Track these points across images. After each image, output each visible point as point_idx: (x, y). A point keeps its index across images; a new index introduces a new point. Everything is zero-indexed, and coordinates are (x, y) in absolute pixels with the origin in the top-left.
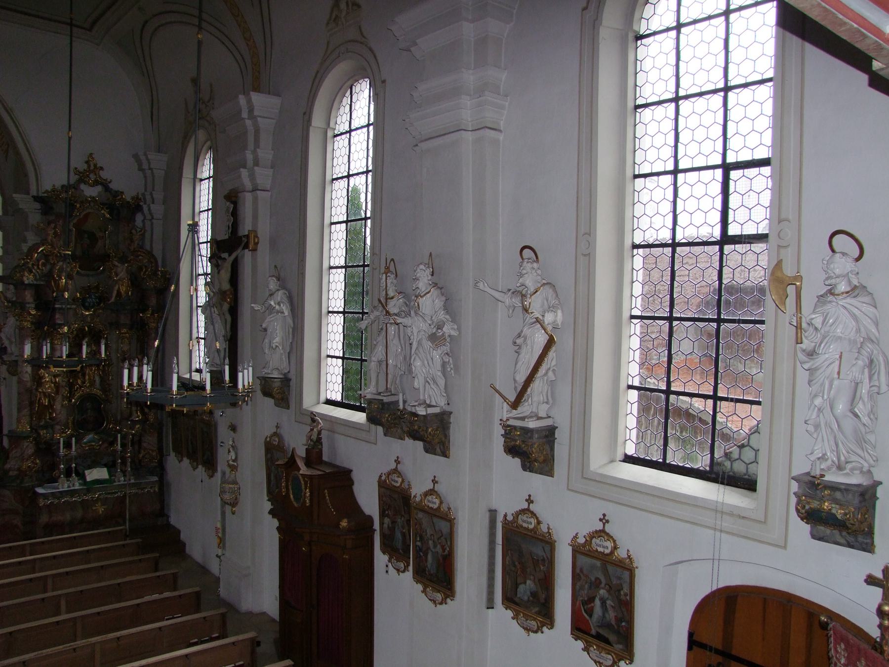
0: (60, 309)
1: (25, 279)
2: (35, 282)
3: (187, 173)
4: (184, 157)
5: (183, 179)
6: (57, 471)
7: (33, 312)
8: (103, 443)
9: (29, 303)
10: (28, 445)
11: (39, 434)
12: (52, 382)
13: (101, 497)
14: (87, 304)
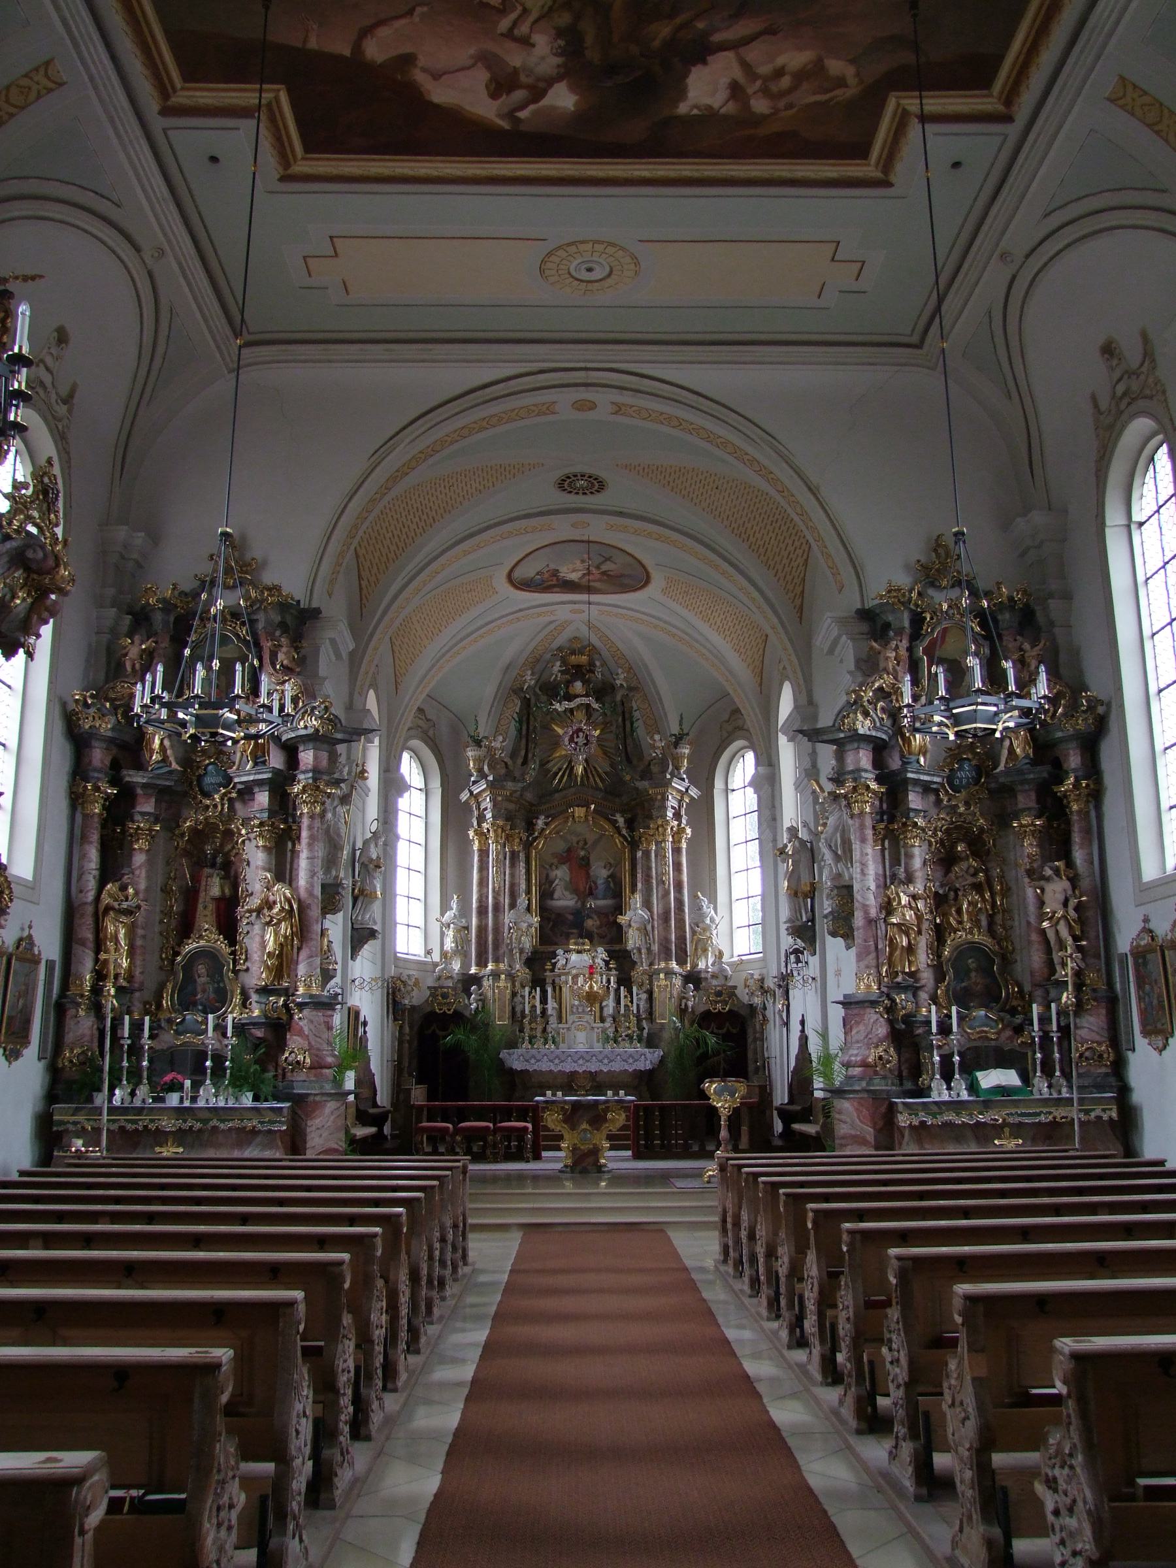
0: (916, 782)
1: (859, 727)
2: (874, 733)
3: (1113, 517)
4: (1104, 498)
5: (1107, 530)
7: (874, 786)
8: (1003, 1029)
9: (866, 771)
11: (893, 1001)
12: (911, 908)
13: (1011, 1120)
14: (957, 782)
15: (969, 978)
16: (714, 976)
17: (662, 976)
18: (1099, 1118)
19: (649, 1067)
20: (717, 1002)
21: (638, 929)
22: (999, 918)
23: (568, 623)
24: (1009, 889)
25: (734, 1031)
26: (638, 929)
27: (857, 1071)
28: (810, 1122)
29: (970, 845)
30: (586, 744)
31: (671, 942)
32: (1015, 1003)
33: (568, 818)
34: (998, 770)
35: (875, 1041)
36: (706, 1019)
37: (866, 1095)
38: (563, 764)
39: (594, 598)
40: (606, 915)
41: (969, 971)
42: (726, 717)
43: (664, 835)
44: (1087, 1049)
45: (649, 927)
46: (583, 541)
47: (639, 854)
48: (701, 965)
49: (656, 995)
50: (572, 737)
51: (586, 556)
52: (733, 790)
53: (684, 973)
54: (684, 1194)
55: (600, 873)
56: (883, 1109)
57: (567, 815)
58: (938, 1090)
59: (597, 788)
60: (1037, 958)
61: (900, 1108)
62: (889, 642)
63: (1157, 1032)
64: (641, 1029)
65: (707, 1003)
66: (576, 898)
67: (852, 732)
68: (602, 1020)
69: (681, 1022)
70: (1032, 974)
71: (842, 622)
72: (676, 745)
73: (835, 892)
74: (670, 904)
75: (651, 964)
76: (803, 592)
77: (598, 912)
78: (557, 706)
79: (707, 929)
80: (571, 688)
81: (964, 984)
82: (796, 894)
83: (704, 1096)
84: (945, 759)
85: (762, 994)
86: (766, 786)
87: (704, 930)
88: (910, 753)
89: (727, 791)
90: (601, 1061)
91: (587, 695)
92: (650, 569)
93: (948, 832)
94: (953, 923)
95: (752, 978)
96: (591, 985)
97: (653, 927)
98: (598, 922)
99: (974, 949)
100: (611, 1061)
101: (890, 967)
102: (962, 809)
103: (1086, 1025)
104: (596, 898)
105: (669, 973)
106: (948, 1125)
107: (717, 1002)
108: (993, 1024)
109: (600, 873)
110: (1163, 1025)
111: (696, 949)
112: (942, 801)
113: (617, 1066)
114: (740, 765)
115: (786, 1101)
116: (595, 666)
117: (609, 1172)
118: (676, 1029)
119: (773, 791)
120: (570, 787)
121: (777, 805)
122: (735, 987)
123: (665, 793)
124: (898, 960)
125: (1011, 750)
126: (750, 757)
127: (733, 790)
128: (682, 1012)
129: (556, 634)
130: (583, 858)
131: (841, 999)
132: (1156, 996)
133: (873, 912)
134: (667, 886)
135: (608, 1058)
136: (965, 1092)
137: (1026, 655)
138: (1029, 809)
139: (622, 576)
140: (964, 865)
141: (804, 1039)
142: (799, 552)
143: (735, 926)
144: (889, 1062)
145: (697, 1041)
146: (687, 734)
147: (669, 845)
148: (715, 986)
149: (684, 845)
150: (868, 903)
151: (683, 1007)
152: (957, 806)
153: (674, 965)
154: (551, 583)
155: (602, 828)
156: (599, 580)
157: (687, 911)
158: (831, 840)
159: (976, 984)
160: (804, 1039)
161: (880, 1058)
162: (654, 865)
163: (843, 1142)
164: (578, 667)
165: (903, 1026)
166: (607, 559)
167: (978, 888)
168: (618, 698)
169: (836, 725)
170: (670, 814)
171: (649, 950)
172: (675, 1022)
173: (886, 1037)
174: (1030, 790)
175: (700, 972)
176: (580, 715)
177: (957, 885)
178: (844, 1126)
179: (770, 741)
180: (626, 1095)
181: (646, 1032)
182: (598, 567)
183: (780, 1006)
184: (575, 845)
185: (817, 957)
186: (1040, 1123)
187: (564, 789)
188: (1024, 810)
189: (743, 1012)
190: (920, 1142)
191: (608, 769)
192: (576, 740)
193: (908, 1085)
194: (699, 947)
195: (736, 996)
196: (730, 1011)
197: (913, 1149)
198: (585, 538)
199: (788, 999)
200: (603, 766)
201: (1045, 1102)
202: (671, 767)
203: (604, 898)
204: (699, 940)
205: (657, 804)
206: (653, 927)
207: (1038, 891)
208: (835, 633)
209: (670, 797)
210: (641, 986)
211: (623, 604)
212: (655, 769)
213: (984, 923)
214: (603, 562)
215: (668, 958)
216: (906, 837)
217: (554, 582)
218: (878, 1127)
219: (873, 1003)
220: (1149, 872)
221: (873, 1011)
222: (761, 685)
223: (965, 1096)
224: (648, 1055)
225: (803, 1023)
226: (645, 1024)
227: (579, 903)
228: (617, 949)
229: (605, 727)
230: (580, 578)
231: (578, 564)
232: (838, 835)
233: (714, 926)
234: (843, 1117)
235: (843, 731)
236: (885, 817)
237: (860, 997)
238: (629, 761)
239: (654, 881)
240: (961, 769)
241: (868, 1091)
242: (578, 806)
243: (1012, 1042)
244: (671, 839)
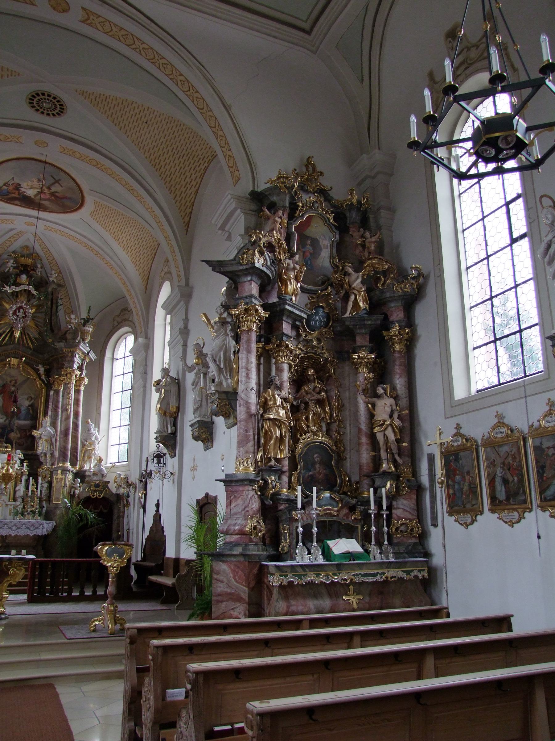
2: (265, 269)
6: (283, 544)
8: (342, 508)
10: (253, 496)
11: (266, 482)
13: (356, 580)
14: (312, 323)
15: (315, 469)
16: (95, 474)
17: (60, 472)
18: (416, 577)
19: (45, 533)
20: (95, 491)
21: (46, 440)
22: (335, 426)
23: (22, 233)
24: (343, 405)
25: (105, 511)
26: (46, 440)
27: (235, 538)
28: (161, 574)
29: (316, 372)
30: (23, 317)
31: (68, 450)
32: (345, 489)
33: (6, 364)
34: (345, 316)
35: (251, 513)
36: (88, 502)
37: (242, 559)
38: (7, 329)
39: (42, 214)
40: (25, 431)
41: (314, 464)
42: (118, 313)
43: (70, 379)
44: (402, 524)
45: (54, 440)
46: (41, 161)
47: (52, 393)
48: (86, 467)
49: (54, 484)
50: (15, 311)
51: (42, 176)
52: (117, 359)
53: (75, 471)
54: (73, 644)
55: (24, 403)
56: (255, 571)
57: (4, 362)
58: (301, 555)
59: (29, 347)
60: (366, 456)
61: (272, 570)
62: (277, 211)
63: (465, 511)
64: (42, 507)
65: (88, 491)
66: (5, 418)
67: (250, 265)
68: (15, 500)
69: (70, 503)
70: (361, 468)
71: (238, 199)
72: (84, 325)
73: (217, 396)
74: (69, 424)
75: (53, 464)
76: (191, 213)
77: (21, 429)
78: (8, 289)
79: (92, 443)
80: (18, 278)
81: (310, 473)
82: (165, 413)
83: (96, 555)
84: (307, 305)
85: (127, 486)
86: (143, 351)
87: (91, 444)
88: (286, 293)
89: (113, 359)
90: (10, 528)
91: (29, 285)
92: (85, 194)
93: (302, 360)
94: (305, 427)
95: (120, 477)
96: (8, 468)
97: (56, 440)
98: (19, 435)
99: (320, 447)
100: (18, 528)
101: (264, 454)
102: (315, 343)
103: (401, 507)
104: (19, 419)
105: (65, 470)
106: (311, 584)
107: (95, 491)
108: (334, 503)
109: (24, 403)
110: (473, 505)
111: (84, 456)
112: (301, 335)
113: (22, 532)
114: (123, 344)
115: (139, 559)
116: (37, 267)
117: (6, 618)
118: (67, 508)
119: (147, 355)
120: (10, 344)
121: (149, 364)
122: (108, 482)
123: (74, 352)
124: (272, 447)
125: (356, 302)
126: (131, 339)
127: (117, 359)
128: (72, 497)
129: (13, 241)
130: (13, 392)
131: (223, 477)
132: (467, 484)
133: (253, 409)
134: (69, 413)
135: (16, 526)
136: (321, 557)
137: (366, 241)
138: (366, 346)
139: (65, 198)
140: (311, 386)
141: (158, 517)
142: (194, 183)
143: (109, 445)
144: (260, 531)
145: (80, 516)
146: (92, 319)
147: (73, 386)
148: (96, 480)
149: (82, 389)
150: (250, 401)
151: (72, 493)
152: (311, 341)
153: (68, 465)
154: (13, 195)
155: (29, 374)
156: (48, 200)
157: (80, 431)
158: (216, 357)
159: (320, 473)
160: (158, 517)
161: (255, 528)
162: (61, 400)
163: (220, 598)
164: (25, 266)
165: (271, 502)
166: (57, 181)
167: (320, 403)
168: (50, 290)
169: (237, 259)
170: (76, 366)
171: (52, 455)
172: (66, 503)
173: (258, 511)
174: (366, 333)
175: (85, 471)
176: (23, 299)
177: (307, 400)
178: (220, 585)
179: (148, 326)
180: (27, 553)
181: (45, 509)
182: (49, 188)
183: (140, 495)
184: (9, 383)
185: (176, 459)
186: (375, 582)
187: (6, 345)
188: (361, 347)
189: (112, 499)
190: (286, 598)
191: (37, 336)
192: (18, 314)
193: (272, 552)
194: (86, 455)
195: (108, 488)
196: (103, 497)
197: (282, 605)
198: (43, 159)
199: (145, 489)
200: (33, 333)
201: (381, 565)
202: (79, 337)
203: (24, 420)
204: (86, 450)
205: (68, 359)
206: (56, 440)
207: (370, 405)
208: (233, 206)
209: (77, 356)
210: (44, 478)
211: (61, 223)
212: (69, 336)
213: (324, 429)
214: (53, 184)
215: (64, 460)
216: (279, 356)
217: (16, 195)
218: (251, 586)
219: (251, 482)
220: (459, 393)
221: (250, 488)
222: (146, 288)
223: (321, 560)
224: (45, 525)
225: (158, 505)
226: (44, 504)
227: (7, 421)
228: (30, 453)
229: (38, 307)
230: (35, 196)
231: (36, 183)
232: (222, 353)
233: (97, 442)
234: (220, 577)
235: (241, 265)
236: (263, 340)
237: (241, 477)
238: (52, 330)
239: (60, 411)
240: (317, 313)
241: (244, 555)
242: (14, 358)
243: (348, 518)
244: (74, 383)
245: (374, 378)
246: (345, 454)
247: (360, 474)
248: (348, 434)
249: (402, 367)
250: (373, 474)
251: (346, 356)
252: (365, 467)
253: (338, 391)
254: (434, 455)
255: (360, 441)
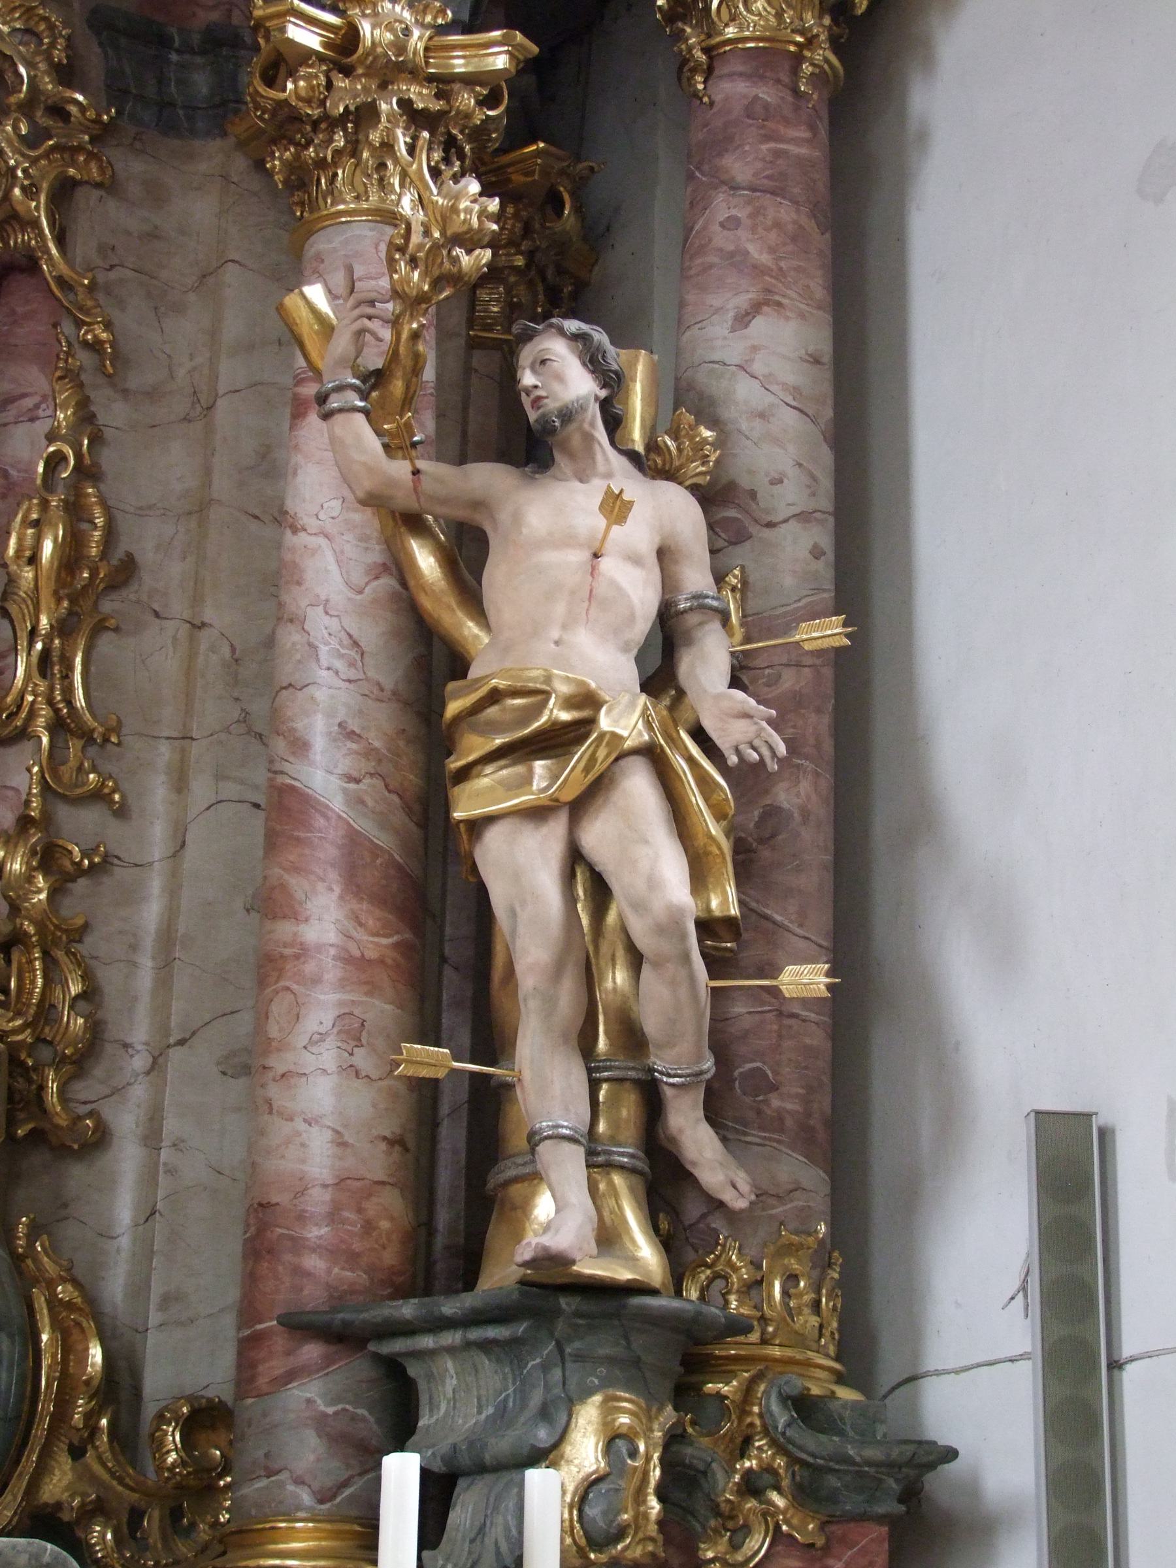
245: (494, 243)
246: (83, 1090)
247: (248, 1312)
248: (156, 885)
249: (785, 212)
250: (408, 1310)
251: (202, 83)
252: (316, 1232)
253: (86, 417)
254: (1106, 1135)
255: (284, 929)
